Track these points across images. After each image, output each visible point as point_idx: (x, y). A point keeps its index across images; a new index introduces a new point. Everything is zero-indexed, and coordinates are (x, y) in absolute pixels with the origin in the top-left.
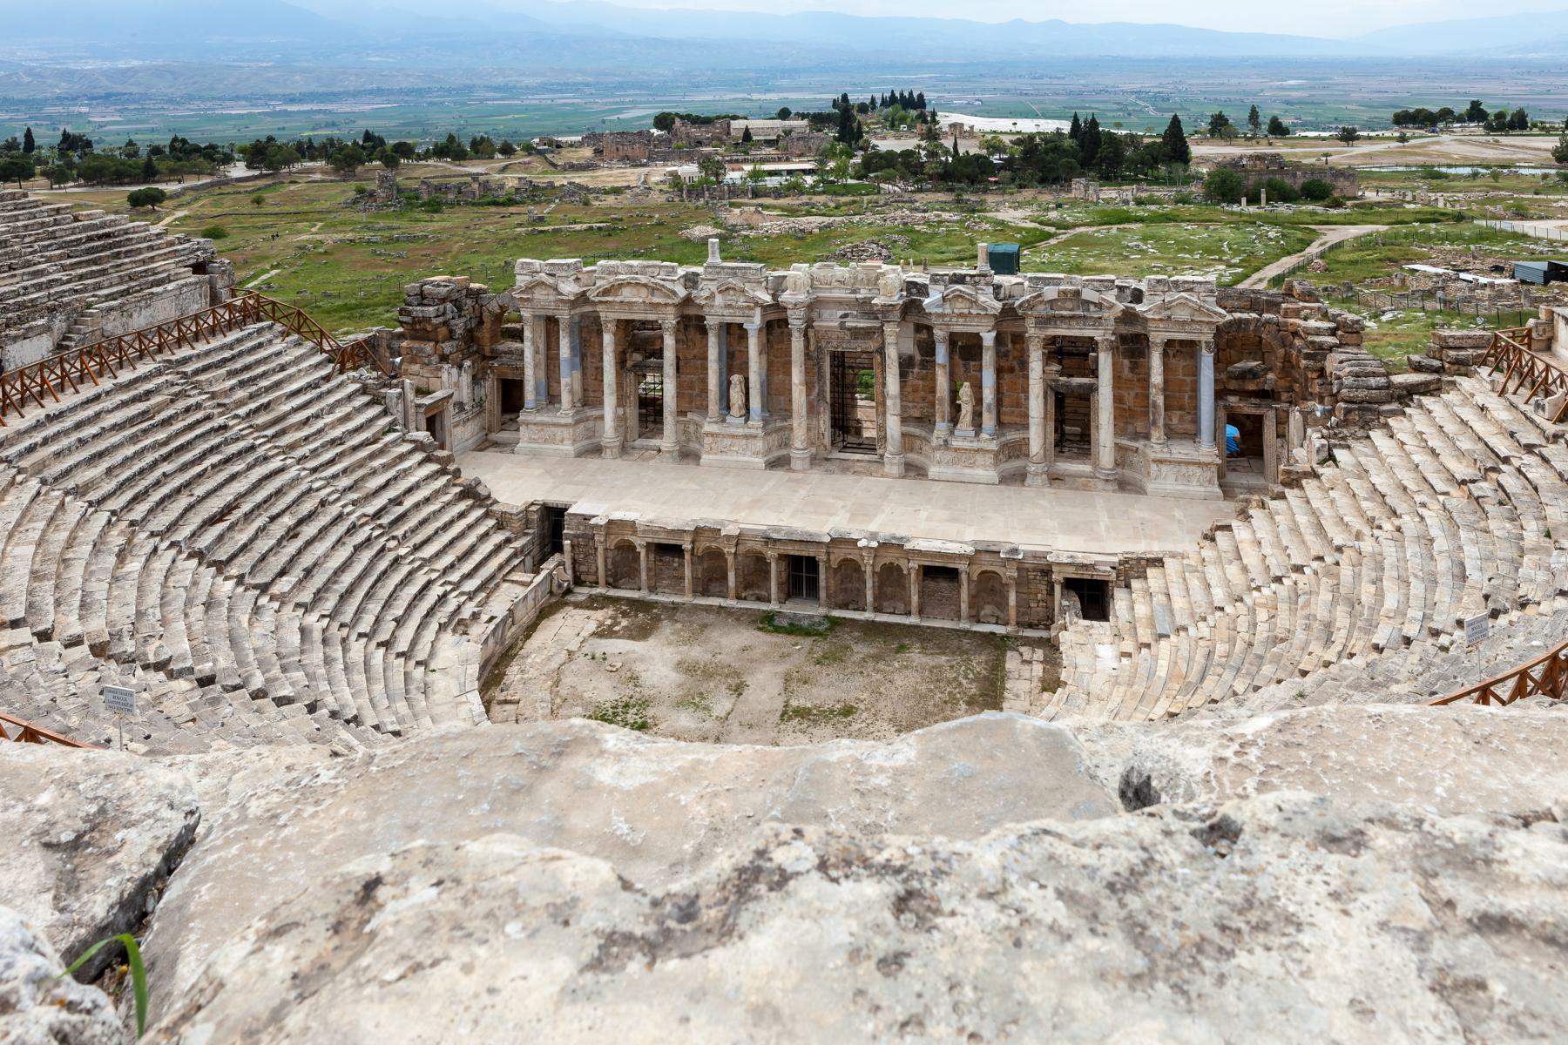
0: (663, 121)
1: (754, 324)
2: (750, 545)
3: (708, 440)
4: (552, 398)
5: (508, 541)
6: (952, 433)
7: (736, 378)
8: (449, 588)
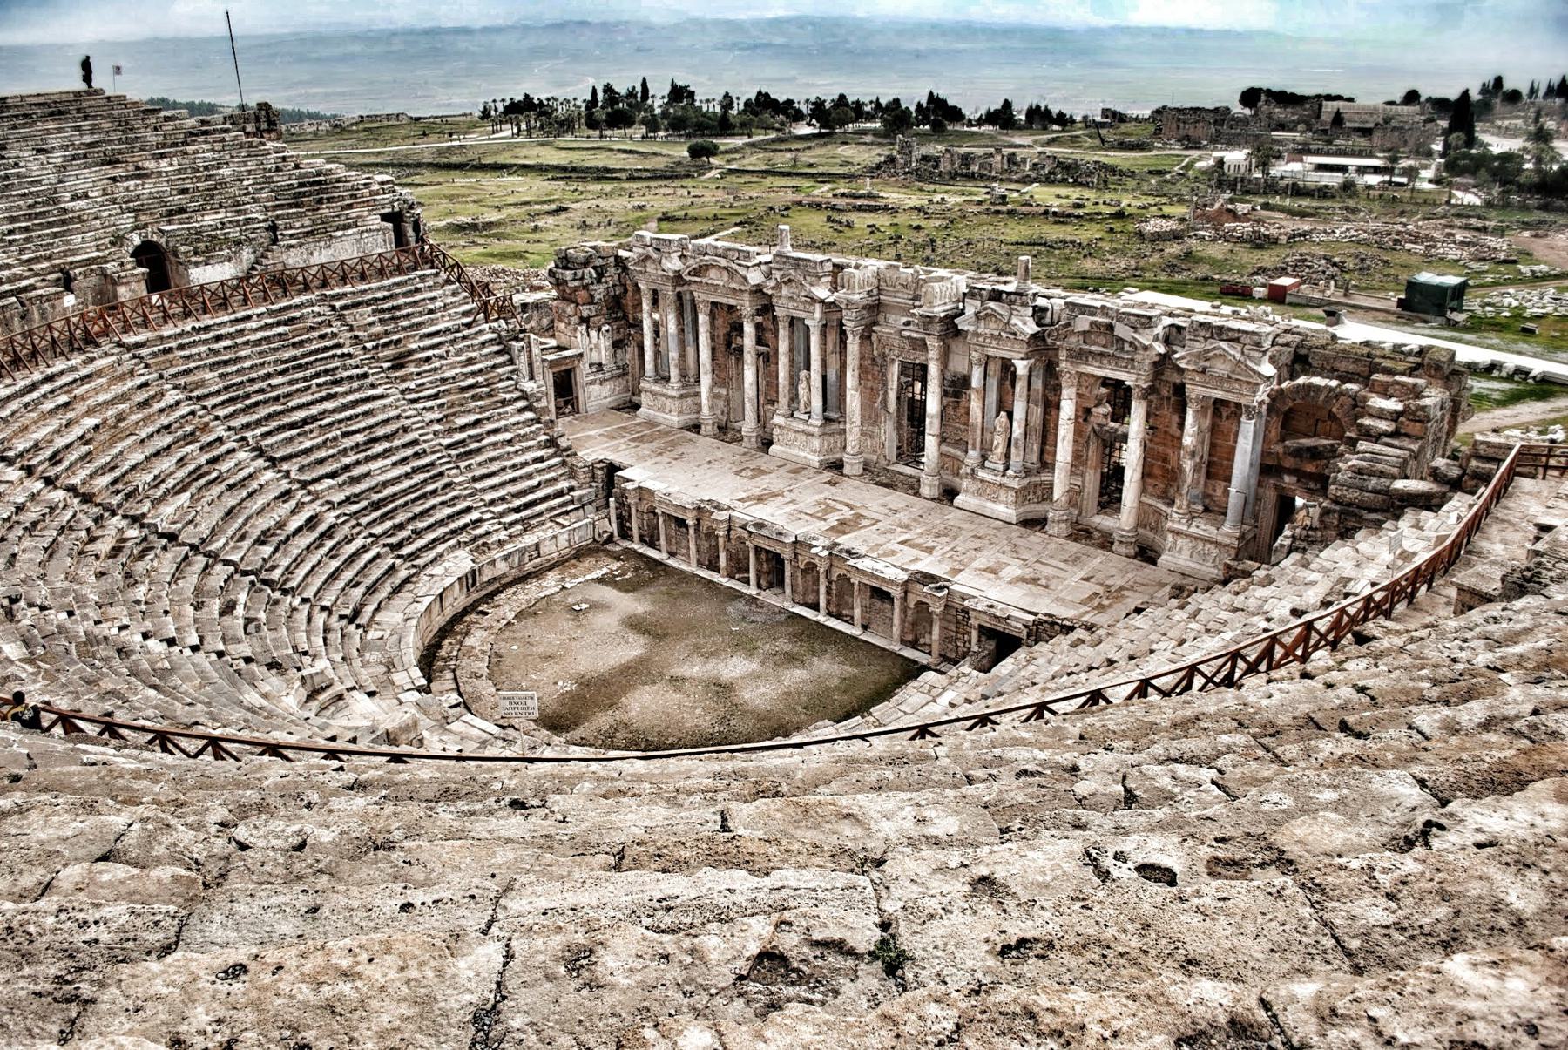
0: (1250, 97)
5: (572, 489)
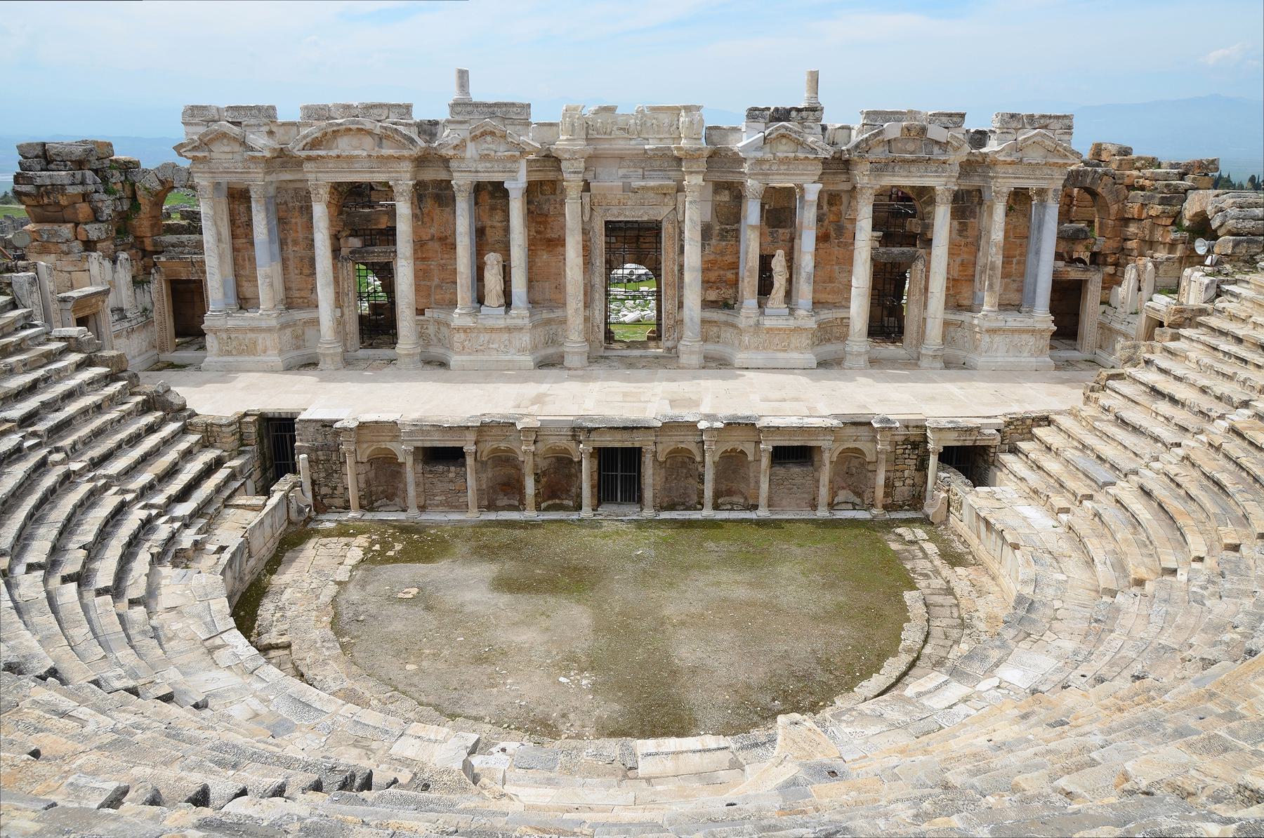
1: (516, 186)
2: (552, 441)
3: (458, 337)
4: (244, 302)
5: (218, 463)
6: (763, 313)
7: (492, 259)
8: (154, 512)
